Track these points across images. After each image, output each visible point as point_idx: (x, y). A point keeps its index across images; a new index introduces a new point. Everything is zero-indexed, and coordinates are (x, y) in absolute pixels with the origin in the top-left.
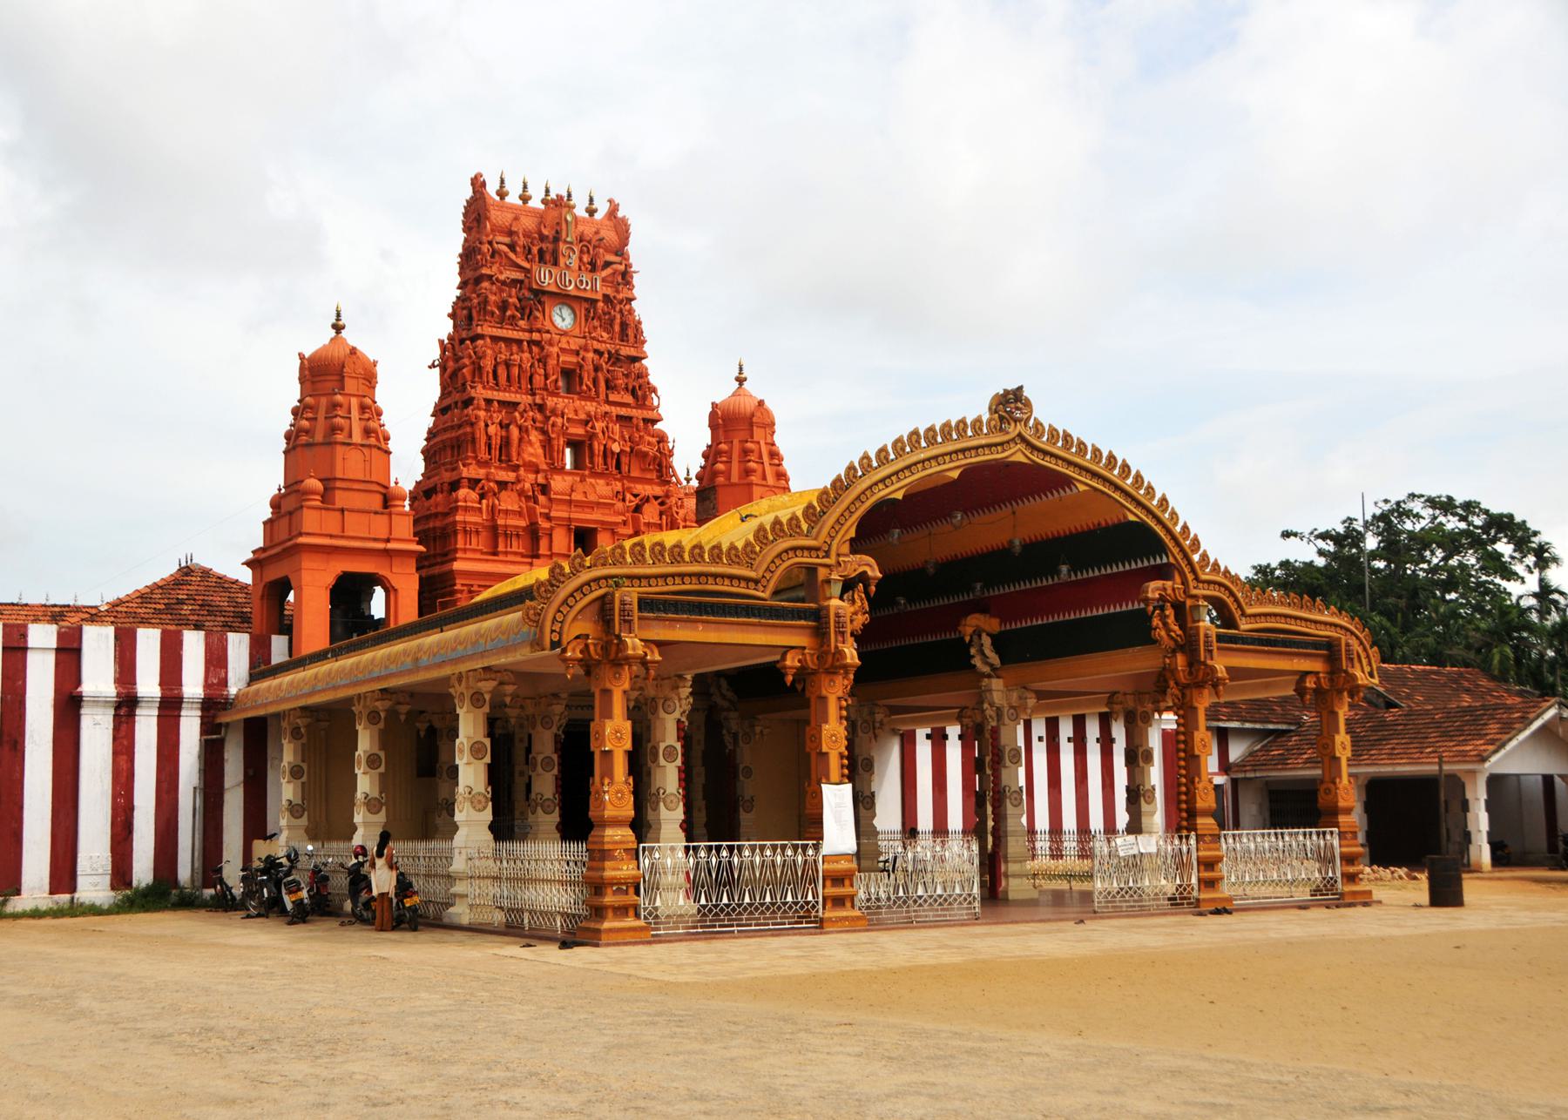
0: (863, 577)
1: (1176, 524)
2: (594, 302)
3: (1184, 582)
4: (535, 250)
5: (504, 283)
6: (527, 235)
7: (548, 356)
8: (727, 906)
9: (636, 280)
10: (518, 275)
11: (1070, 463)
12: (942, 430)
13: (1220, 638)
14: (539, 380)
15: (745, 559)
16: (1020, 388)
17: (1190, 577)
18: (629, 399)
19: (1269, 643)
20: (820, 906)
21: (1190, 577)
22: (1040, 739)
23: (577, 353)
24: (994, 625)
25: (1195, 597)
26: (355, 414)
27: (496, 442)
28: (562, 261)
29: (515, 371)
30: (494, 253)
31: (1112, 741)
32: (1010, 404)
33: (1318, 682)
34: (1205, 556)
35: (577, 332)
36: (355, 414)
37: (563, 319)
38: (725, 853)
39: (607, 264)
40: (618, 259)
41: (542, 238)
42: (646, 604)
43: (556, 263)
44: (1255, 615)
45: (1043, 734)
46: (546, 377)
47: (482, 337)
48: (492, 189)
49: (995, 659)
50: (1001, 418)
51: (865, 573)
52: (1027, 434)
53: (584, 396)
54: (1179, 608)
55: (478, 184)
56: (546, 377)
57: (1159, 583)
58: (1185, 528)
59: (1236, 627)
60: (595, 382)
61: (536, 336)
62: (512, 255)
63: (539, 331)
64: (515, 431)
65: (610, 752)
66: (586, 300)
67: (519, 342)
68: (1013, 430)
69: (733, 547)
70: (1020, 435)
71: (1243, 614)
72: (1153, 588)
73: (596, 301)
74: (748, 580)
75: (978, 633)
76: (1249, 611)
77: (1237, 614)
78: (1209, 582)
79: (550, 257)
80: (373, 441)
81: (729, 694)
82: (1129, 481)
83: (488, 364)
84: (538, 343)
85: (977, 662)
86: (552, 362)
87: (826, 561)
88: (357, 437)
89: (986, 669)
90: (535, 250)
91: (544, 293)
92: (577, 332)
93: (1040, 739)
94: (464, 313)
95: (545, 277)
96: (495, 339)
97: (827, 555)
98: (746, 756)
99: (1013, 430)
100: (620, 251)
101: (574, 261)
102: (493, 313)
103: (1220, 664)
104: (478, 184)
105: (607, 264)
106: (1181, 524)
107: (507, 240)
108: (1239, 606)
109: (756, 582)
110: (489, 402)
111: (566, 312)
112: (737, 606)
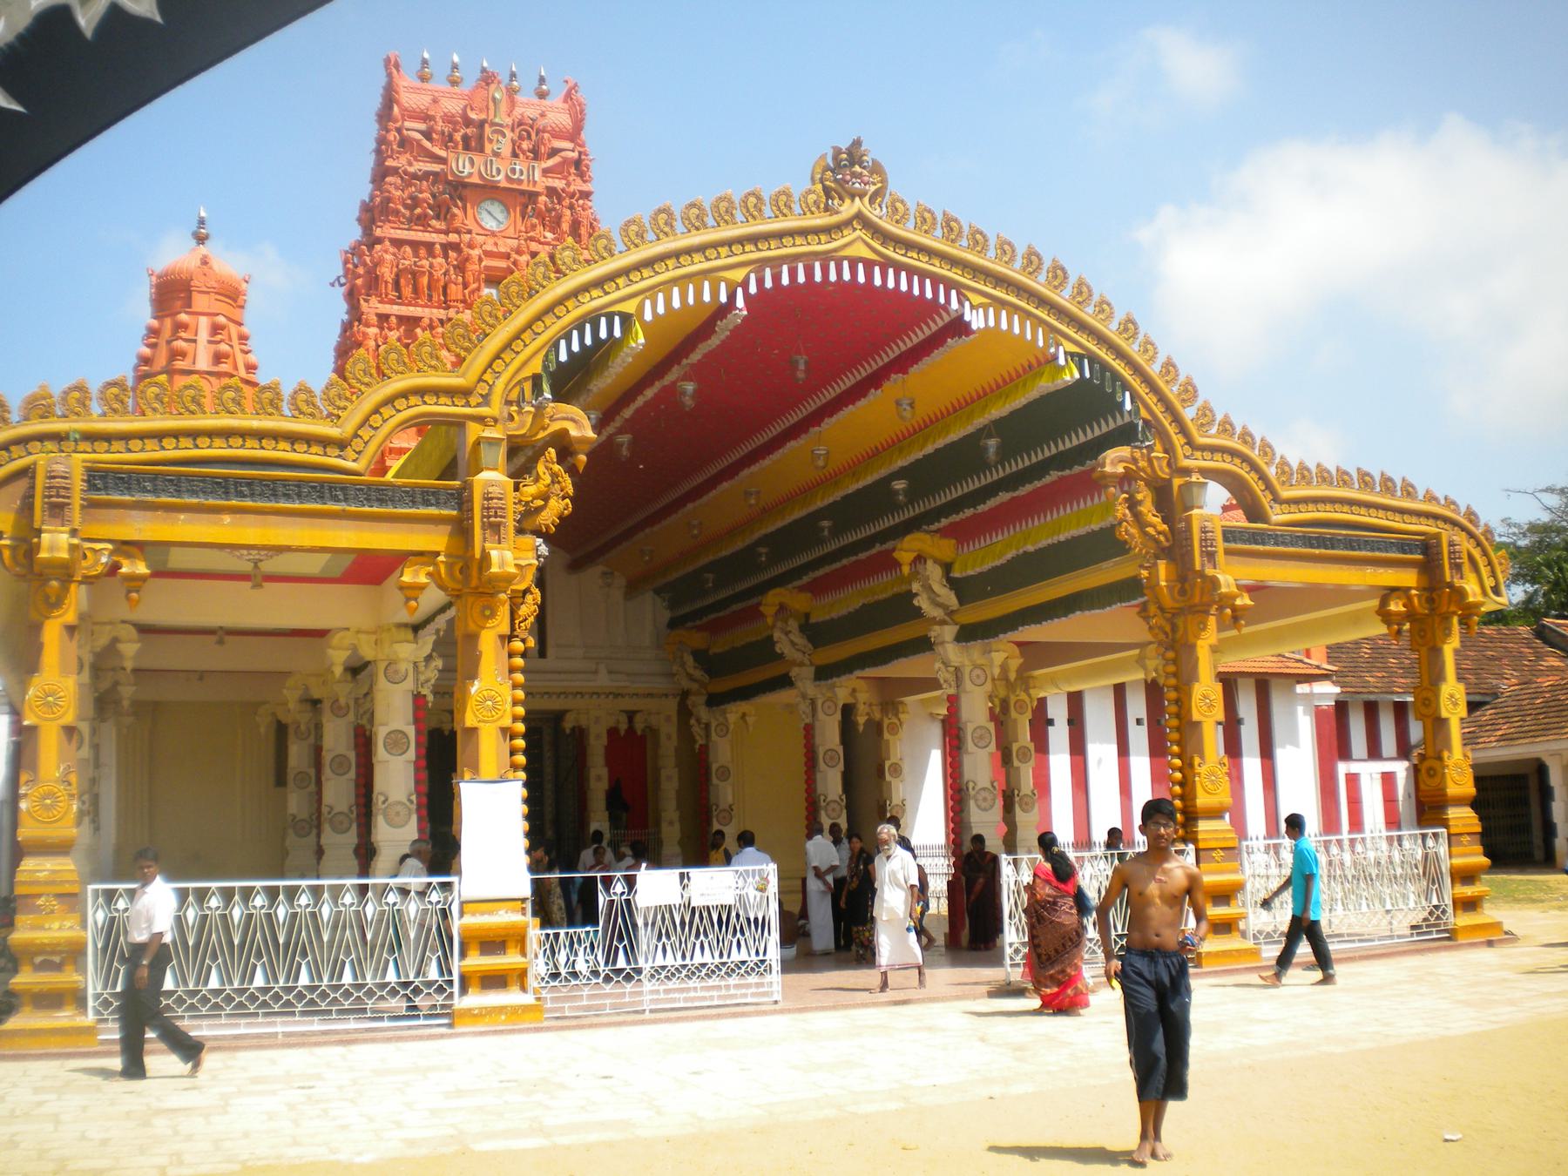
1: (1152, 359)
2: (532, 196)
3: (1169, 449)
4: (458, 137)
5: (414, 176)
6: (449, 119)
7: (467, 259)
8: (264, 990)
9: (595, 170)
10: (436, 168)
11: (954, 262)
12: (716, 207)
13: (1229, 535)
14: (455, 291)
15: (325, 409)
16: (857, 143)
17: (1178, 440)
19: (1322, 542)
20: (456, 988)
21: (1178, 440)
22: (1139, 722)
23: (507, 256)
24: (945, 548)
25: (1186, 472)
28: (488, 148)
29: (425, 280)
30: (405, 143)
31: (1239, 722)
32: (846, 169)
33: (1408, 604)
34: (1206, 411)
35: (511, 232)
36: (203, 335)
37: (492, 218)
38: (259, 901)
39: (554, 152)
40: (569, 145)
41: (468, 122)
42: (98, 478)
43: (482, 150)
44: (1296, 501)
45: (1143, 715)
46: (465, 286)
47: (379, 241)
49: (951, 599)
50: (827, 191)
51: (565, 432)
52: (875, 214)
54: (1162, 494)
55: (391, 65)
56: (465, 286)
57: (1124, 451)
58: (1169, 366)
59: (1265, 520)
61: (453, 237)
62: (427, 144)
63: (458, 232)
65: (33, 729)
66: (523, 192)
67: (429, 246)
68: (848, 209)
69: (303, 389)
70: (859, 216)
71: (1276, 499)
72: (1114, 460)
73: (538, 194)
74: (325, 442)
75: (920, 559)
76: (1286, 493)
77: (1265, 499)
78: (1214, 449)
79: (474, 144)
80: (223, 367)
81: (698, 674)
82: (1067, 293)
83: (387, 273)
84: (456, 247)
85: (922, 602)
86: (472, 267)
87: (484, 411)
88: (203, 363)
89: (937, 613)
90: (458, 137)
91: (465, 185)
92: (511, 232)
93: (1139, 722)
94: (371, 215)
95: (465, 166)
96: (398, 243)
97: (486, 400)
98: (722, 753)
99: (848, 209)
100: (574, 135)
101: (505, 148)
102: (397, 213)
103: (1229, 576)
105: (554, 152)
106: (1161, 359)
107: (423, 127)
108: (1269, 486)
109: (342, 445)
110: (383, 318)
111: (496, 209)
112: (300, 483)
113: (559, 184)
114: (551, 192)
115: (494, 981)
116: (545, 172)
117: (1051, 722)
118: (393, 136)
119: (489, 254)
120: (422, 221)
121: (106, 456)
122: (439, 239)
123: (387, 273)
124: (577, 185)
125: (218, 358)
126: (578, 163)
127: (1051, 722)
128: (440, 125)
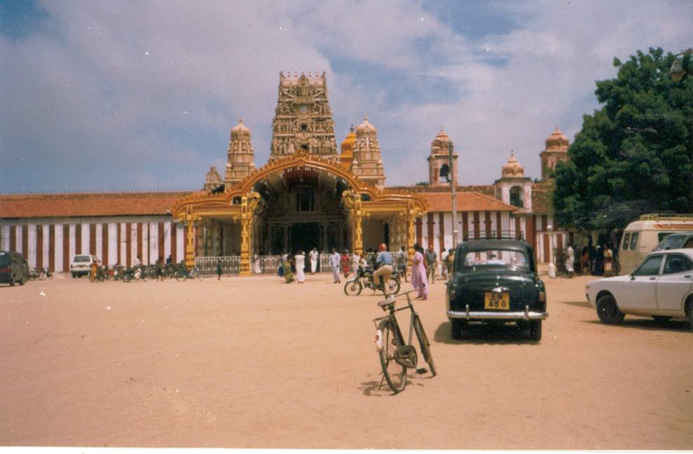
0: (255, 198)
2: (312, 105)
6: (293, 87)
18: (323, 130)
23: (306, 120)
26: (240, 145)
27: (281, 147)
30: (283, 95)
31: (491, 222)
36: (240, 145)
48: (285, 74)
53: (309, 132)
55: (281, 75)
60: (312, 127)
62: (289, 95)
64: (285, 146)
67: (288, 119)
84: (295, 119)
96: (282, 119)
99: (299, 159)
100: (324, 86)
104: (281, 75)
105: (319, 91)
113: (318, 99)
114: (317, 102)
115: (245, 270)
116: (316, 97)
117: (434, 223)
118: (281, 94)
119: (302, 120)
120: (287, 113)
121: (195, 205)
122: (291, 117)
123: (279, 127)
124: (324, 99)
125: (243, 150)
126: (324, 94)
127: (434, 223)
128: (291, 89)
